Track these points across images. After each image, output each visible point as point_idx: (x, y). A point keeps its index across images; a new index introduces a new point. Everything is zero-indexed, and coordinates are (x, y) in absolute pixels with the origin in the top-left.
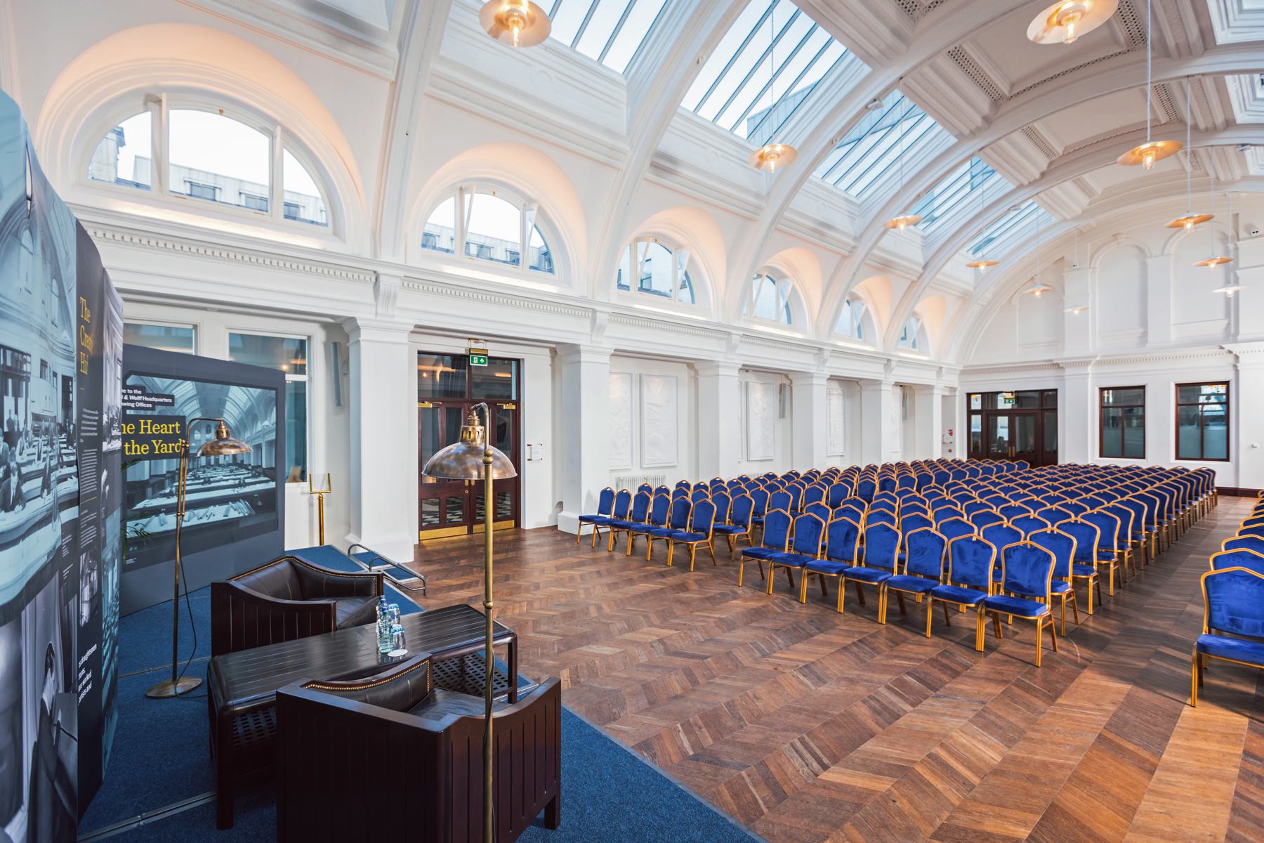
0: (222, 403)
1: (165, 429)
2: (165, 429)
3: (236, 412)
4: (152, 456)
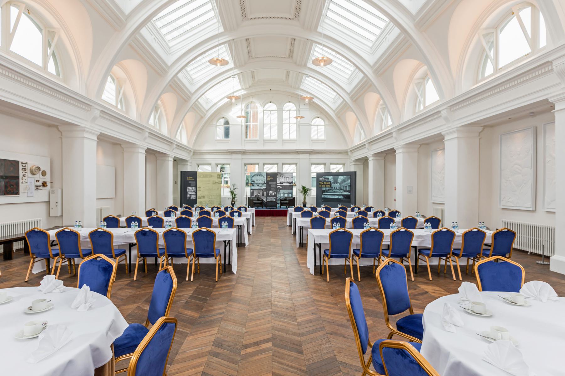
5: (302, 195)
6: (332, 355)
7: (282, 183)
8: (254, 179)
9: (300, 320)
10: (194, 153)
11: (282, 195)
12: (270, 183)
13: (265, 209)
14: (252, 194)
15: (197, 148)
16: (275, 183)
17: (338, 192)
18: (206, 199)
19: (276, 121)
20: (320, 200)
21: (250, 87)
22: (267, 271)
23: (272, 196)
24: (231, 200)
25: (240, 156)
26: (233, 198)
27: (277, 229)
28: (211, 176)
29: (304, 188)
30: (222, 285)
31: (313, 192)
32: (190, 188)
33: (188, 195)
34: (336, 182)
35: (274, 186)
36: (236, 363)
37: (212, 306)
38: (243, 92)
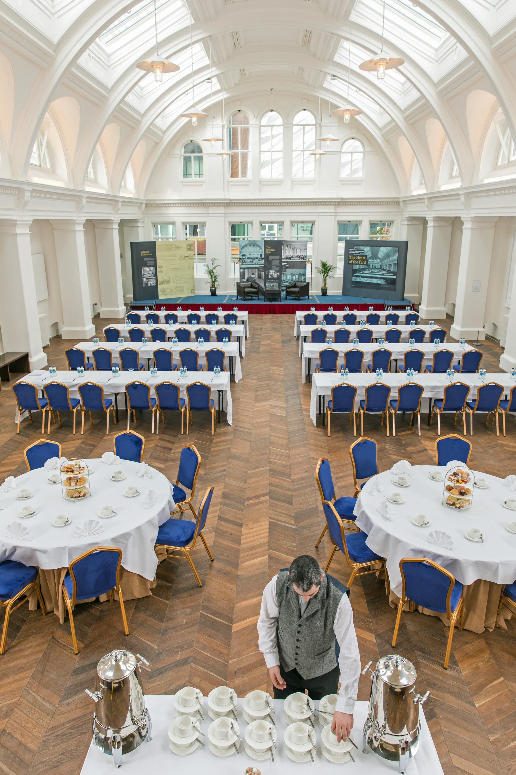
0: (378, 252)
1: (362, 258)
2: (362, 258)
3: (382, 254)
4: (358, 264)
5: (321, 277)
6: (315, 506)
7: (290, 258)
8: (245, 251)
9: (294, 477)
10: (147, 205)
11: (289, 277)
12: (271, 258)
13: (262, 303)
14: (242, 276)
15: (151, 197)
16: (278, 258)
17: (377, 273)
18: (172, 285)
19: (280, 146)
20: (350, 284)
21: (236, 85)
22: (265, 422)
23: (273, 279)
24: (209, 286)
25: (221, 210)
26: (213, 282)
27: (279, 346)
28: (177, 248)
29: (324, 265)
30: (219, 440)
31: (339, 272)
32: (147, 269)
33: (145, 281)
34: (375, 256)
35: (277, 263)
36: (242, 510)
37: (214, 463)
38: (223, 96)
